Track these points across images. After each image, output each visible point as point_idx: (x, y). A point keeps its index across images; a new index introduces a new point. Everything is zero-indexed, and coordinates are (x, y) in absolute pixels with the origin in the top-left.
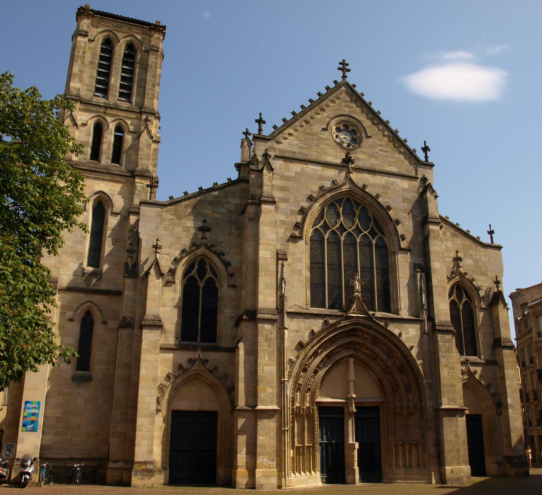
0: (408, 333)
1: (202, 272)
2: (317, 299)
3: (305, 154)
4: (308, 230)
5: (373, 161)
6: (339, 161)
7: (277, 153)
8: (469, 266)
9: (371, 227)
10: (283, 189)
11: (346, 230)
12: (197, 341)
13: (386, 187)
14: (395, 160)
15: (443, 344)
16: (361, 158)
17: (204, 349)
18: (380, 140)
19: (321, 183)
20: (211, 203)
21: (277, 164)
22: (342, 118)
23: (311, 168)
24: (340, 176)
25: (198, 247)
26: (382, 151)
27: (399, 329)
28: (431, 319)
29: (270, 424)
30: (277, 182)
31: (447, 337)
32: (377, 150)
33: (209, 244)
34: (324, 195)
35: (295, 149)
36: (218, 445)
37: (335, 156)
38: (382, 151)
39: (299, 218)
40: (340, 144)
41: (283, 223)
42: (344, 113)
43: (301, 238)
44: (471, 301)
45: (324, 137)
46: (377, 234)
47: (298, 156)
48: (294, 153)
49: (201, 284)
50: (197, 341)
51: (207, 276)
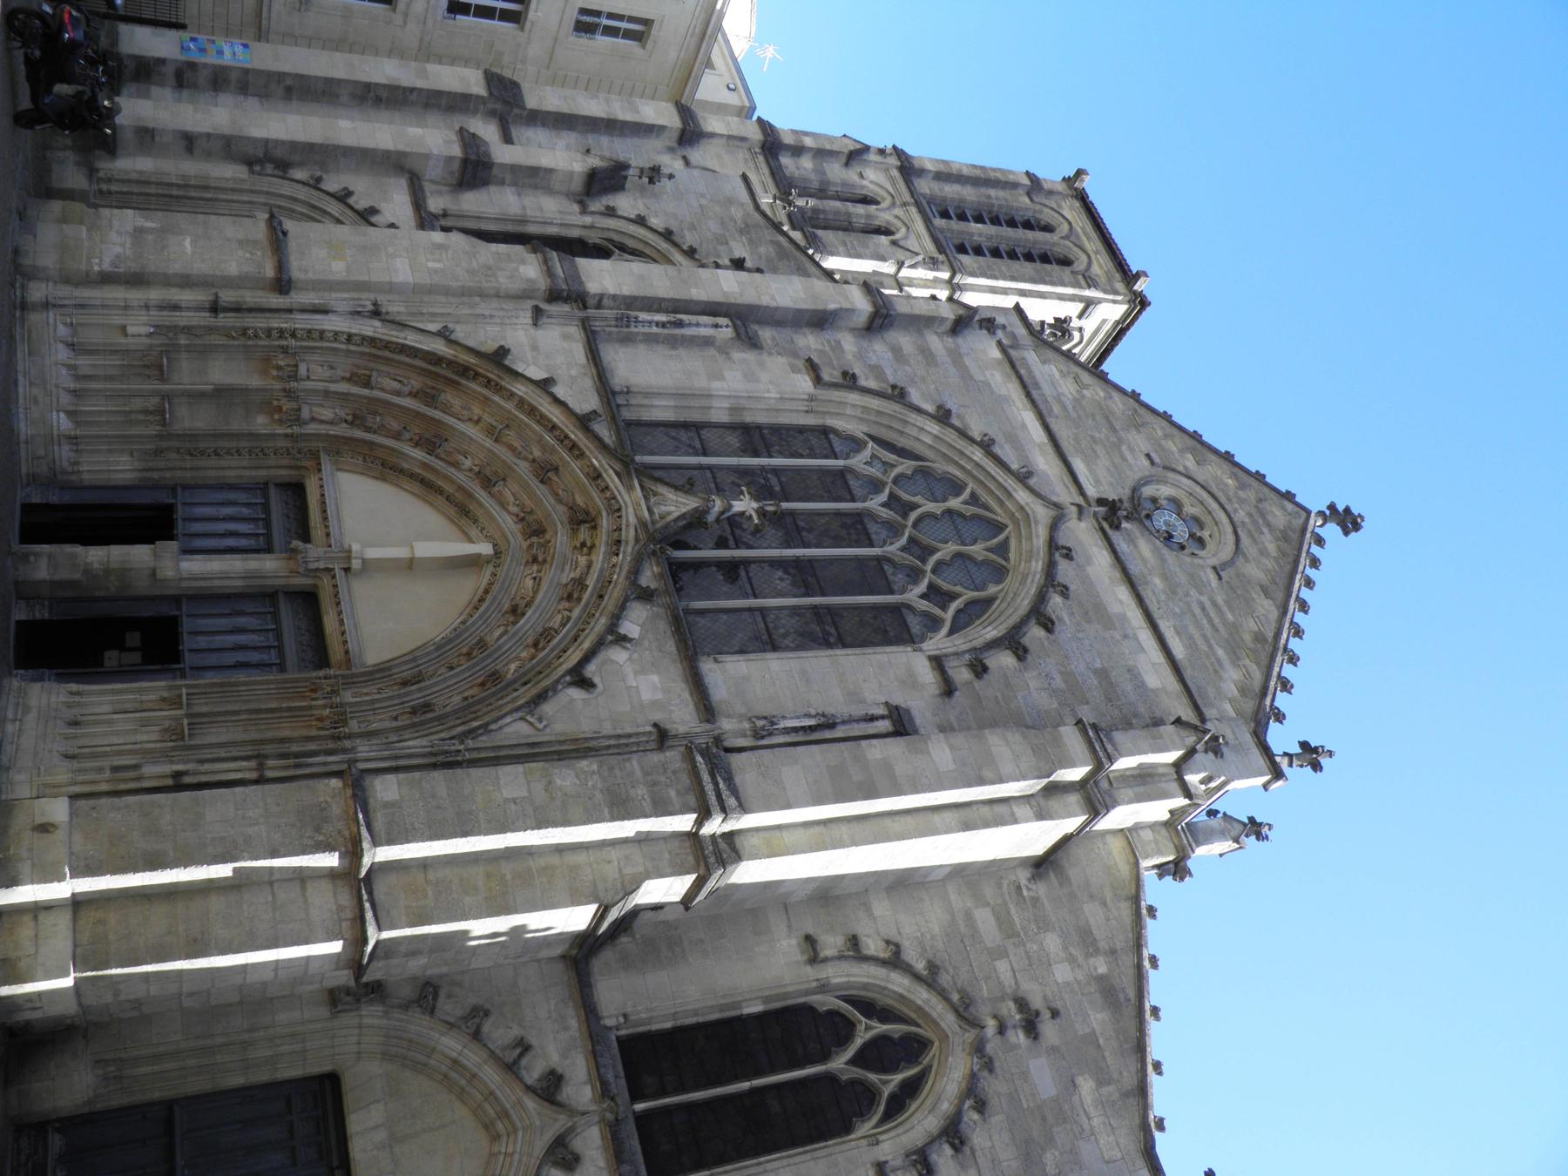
0: (640, 672)
6: (1092, 492)
8: (1025, 1075)
9: (958, 589)
14: (1204, 647)
15: (639, 773)
19: (1000, 438)
22: (1214, 505)
23: (1029, 418)
26: (1203, 609)
27: (642, 637)
29: (234, 264)
31: (673, 793)
38: (1203, 609)
41: (838, 346)
43: (818, 380)
44: (889, 1115)
45: (1129, 458)
47: (1035, 393)
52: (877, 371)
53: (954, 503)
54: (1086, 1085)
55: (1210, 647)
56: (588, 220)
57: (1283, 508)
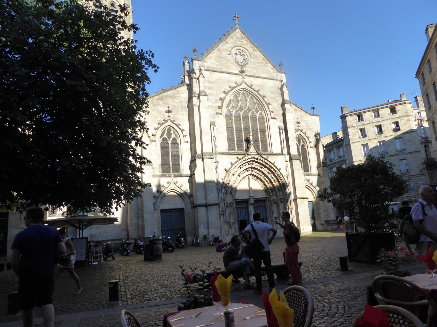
1: (169, 135)
2: (231, 147)
3: (219, 69)
4: (225, 110)
5: (255, 71)
6: (238, 72)
7: (206, 68)
10: (210, 88)
11: (243, 110)
12: (169, 172)
13: (262, 86)
16: (248, 70)
17: (175, 176)
18: (257, 60)
20: (171, 97)
21: (206, 73)
24: (239, 79)
25: (166, 122)
26: (259, 66)
28: (289, 153)
30: (207, 85)
32: (256, 66)
33: (172, 120)
34: (231, 90)
35: (214, 66)
36: (186, 226)
37: (235, 69)
38: (259, 66)
39: (220, 104)
40: (237, 62)
41: (212, 106)
42: (238, 45)
43: (221, 114)
46: (258, 111)
47: (216, 70)
48: (214, 68)
49: (170, 142)
50: (169, 172)
51: (172, 137)
52: (216, 101)
53: (239, 99)
54: (304, 119)
55: (265, 69)
56: (157, 141)
57: (237, 32)
